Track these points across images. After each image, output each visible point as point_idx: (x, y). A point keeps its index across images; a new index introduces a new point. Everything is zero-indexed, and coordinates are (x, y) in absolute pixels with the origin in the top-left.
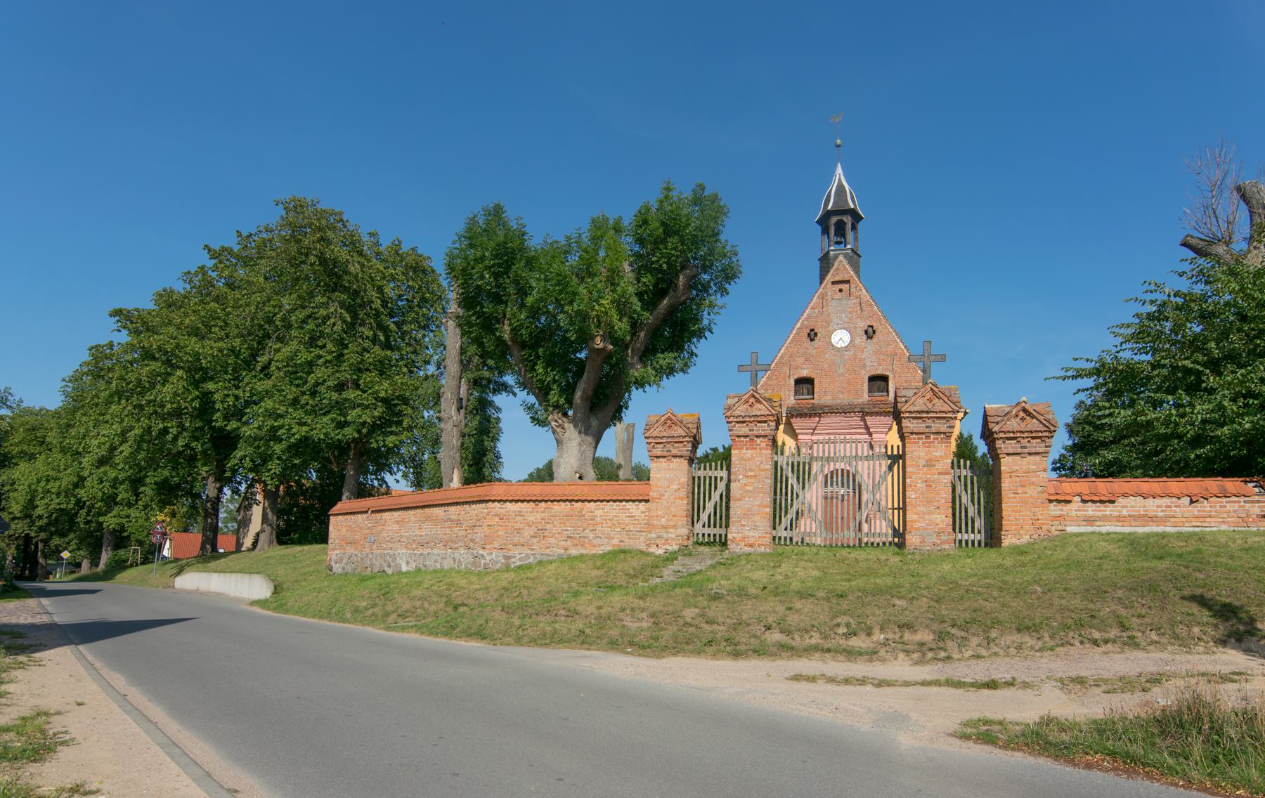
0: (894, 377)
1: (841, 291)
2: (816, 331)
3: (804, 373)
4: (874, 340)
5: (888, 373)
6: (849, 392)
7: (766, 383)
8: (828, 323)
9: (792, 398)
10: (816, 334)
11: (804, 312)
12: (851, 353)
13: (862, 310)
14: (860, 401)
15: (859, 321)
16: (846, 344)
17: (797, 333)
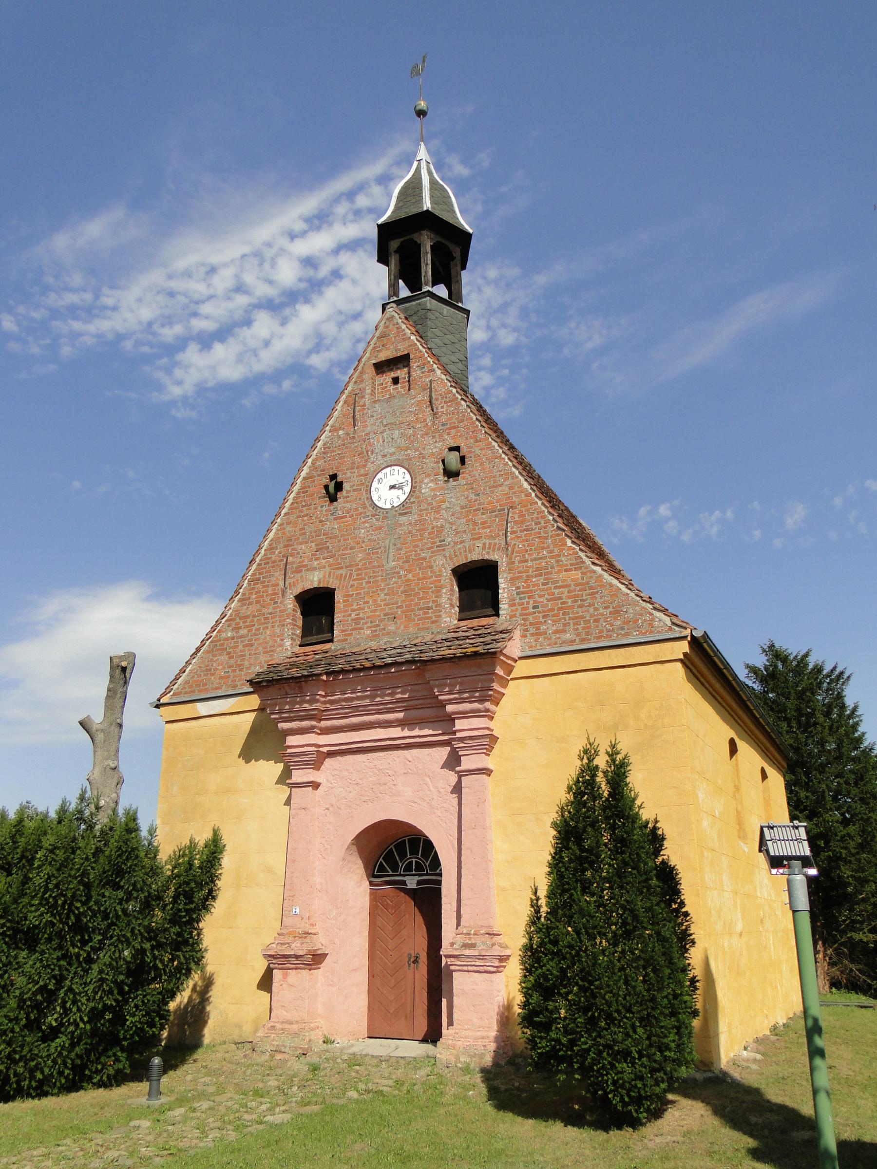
0: (511, 563)
1: (396, 381)
2: (339, 479)
3: (314, 580)
4: (461, 480)
5: (494, 557)
8: (364, 455)
9: (288, 643)
10: (339, 487)
11: (317, 440)
12: (413, 518)
13: (435, 414)
15: (429, 439)
17: (303, 490)
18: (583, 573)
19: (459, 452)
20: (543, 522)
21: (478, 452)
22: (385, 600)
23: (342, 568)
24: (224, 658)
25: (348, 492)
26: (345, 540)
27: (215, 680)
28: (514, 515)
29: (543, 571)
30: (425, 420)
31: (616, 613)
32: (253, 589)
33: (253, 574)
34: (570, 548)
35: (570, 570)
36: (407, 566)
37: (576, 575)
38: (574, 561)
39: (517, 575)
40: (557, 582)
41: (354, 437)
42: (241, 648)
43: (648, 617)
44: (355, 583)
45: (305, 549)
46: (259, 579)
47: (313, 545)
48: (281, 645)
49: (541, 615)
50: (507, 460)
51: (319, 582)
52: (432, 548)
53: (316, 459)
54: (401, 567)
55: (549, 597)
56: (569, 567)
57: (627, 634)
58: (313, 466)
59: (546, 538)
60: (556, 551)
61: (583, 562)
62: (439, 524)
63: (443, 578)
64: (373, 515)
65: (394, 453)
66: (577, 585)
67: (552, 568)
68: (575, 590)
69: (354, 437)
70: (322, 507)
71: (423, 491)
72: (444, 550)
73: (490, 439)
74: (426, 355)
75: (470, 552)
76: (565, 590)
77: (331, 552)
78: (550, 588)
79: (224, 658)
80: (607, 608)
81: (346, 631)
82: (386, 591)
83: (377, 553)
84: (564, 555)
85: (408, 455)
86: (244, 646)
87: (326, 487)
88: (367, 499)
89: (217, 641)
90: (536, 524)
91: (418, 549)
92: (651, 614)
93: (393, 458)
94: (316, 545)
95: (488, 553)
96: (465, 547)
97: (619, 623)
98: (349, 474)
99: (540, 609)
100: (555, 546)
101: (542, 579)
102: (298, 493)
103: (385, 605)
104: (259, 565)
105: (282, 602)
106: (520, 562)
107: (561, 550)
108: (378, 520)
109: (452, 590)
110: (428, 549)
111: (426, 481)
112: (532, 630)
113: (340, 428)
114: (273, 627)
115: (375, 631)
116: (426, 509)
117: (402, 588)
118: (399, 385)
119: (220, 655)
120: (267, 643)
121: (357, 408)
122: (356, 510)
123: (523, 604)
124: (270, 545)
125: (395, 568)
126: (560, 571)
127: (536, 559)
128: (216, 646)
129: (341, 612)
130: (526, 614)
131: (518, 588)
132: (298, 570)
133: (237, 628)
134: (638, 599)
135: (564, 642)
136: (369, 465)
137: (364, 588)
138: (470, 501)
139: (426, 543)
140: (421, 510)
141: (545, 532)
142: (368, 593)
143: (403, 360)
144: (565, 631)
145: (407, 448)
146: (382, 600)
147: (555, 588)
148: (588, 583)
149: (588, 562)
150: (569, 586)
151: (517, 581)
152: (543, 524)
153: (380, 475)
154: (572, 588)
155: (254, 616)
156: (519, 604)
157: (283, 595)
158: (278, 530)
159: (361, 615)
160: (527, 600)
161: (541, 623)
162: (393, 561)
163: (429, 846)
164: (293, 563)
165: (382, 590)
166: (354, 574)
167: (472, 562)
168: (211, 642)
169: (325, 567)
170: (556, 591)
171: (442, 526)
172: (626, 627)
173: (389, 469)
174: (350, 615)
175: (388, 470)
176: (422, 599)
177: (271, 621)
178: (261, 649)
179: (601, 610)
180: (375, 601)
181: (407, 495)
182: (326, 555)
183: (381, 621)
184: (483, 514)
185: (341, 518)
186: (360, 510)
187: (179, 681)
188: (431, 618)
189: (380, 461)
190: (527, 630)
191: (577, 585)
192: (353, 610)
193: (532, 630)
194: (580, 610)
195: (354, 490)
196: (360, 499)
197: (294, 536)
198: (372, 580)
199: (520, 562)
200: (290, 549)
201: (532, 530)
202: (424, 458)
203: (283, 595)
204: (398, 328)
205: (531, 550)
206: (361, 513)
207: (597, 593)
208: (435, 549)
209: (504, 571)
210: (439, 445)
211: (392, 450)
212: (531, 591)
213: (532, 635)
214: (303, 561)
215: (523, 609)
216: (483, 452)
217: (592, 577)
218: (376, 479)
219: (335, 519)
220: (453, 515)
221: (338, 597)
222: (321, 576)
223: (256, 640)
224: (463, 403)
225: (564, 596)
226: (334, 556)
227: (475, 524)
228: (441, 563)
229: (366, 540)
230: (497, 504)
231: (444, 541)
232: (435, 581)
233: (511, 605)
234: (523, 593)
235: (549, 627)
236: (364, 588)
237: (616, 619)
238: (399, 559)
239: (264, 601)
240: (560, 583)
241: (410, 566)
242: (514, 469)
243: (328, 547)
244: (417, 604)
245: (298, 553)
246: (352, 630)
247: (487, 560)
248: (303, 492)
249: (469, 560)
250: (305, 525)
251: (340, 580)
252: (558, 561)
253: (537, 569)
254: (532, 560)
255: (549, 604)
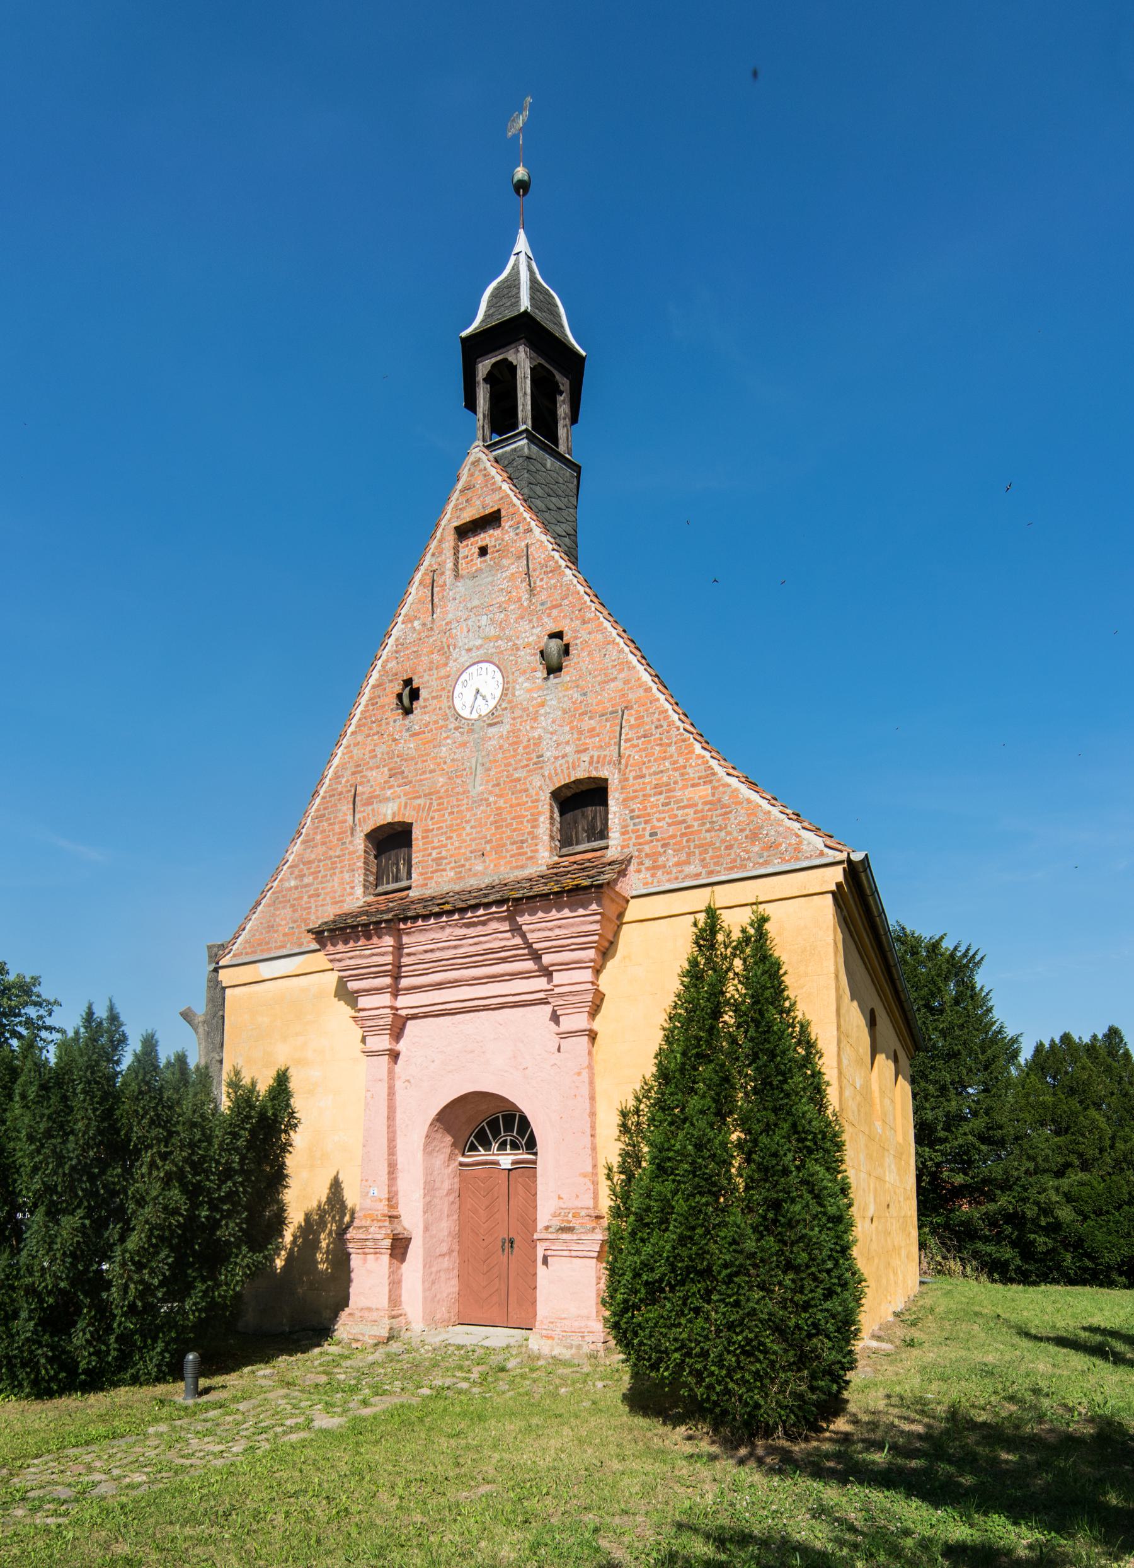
1: (483, 551)
2: (415, 685)
3: (387, 813)
4: (565, 676)
5: (603, 773)
6: (499, 848)
7: (300, 857)
8: (445, 651)
9: (359, 891)
10: (415, 695)
12: (504, 729)
13: (532, 590)
14: (531, 871)
15: (524, 625)
16: (492, 703)
17: (373, 701)
18: (714, 788)
19: (562, 639)
20: (665, 724)
21: (587, 637)
22: (471, 834)
23: (420, 797)
24: (287, 912)
25: (425, 700)
26: (424, 761)
27: (278, 937)
28: (630, 718)
29: (664, 789)
30: (520, 599)
31: (754, 836)
32: (317, 827)
33: (317, 810)
34: (699, 756)
35: (698, 785)
36: (497, 790)
37: (705, 791)
38: (703, 774)
39: (632, 794)
40: (682, 801)
41: (432, 629)
42: (306, 899)
43: (794, 840)
44: (436, 815)
45: (377, 777)
46: (324, 815)
47: (386, 769)
48: (352, 894)
49: (659, 844)
50: (622, 645)
51: (394, 815)
52: (527, 766)
53: (387, 661)
54: (491, 792)
55: (670, 821)
56: (696, 781)
57: (766, 863)
58: (384, 671)
59: (669, 745)
60: (681, 761)
61: (714, 774)
62: (536, 735)
63: (541, 803)
64: (456, 729)
65: (481, 646)
66: (705, 803)
67: (676, 783)
68: (702, 811)
69: (432, 629)
70: (395, 721)
71: (517, 693)
72: (541, 768)
73: (602, 619)
74: (522, 509)
75: (574, 768)
76: (690, 811)
77: (407, 777)
78: (672, 810)
79: (287, 912)
80: (742, 830)
81: (426, 873)
82: (472, 823)
83: (461, 776)
84: (691, 766)
85: (499, 647)
86: (310, 897)
87: (400, 696)
88: (449, 708)
89: (279, 892)
90: (657, 727)
91: (510, 768)
92: (797, 836)
93: (481, 652)
94: (390, 770)
95: (596, 769)
96: (567, 762)
97: (756, 849)
98: (426, 678)
99: (659, 836)
100: (680, 754)
101: (662, 798)
102: (367, 706)
103: (471, 840)
104: (324, 798)
105: (351, 842)
106: (635, 778)
107: (687, 760)
108: (462, 733)
109: (552, 818)
110: (523, 767)
111: (520, 680)
112: (648, 863)
113: (416, 618)
114: (342, 872)
115: (460, 872)
116: (521, 717)
117: (492, 819)
118: (488, 557)
119: (284, 908)
120: (335, 892)
121: (436, 590)
122: (436, 722)
123: (638, 831)
124: (335, 773)
125: (482, 793)
126: (684, 787)
127: (655, 773)
128: (278, 898)
129: (420, 851)
130: (640, 844)
131: (633, 811)
132: (369, 803)
133: (301, 876)
134: (784, 816)
135: (686, 877)
136: (451, 663)
137: (446, 821)
138: (574, 703)
139: (520, 761)
140: (514, 719)
141: (669, 738)
142: (451, 826)
143: (491, 520)
144: (689, 863)
145: (498, 638)
146: (468, 835)
147: (679, 808)
148: (719, 800)
149: (721, 772)
150: (696, 805)
151: (631, 803)
152: (665, 727)
153: (464, 676)
154: (700, 807)
155: (320, 861)
156: (634, 831)
157: (352, 834)
158: (344, 754)
159: (443, 854)
160: (643, 825)
161: (660, 854)
162: (481, 785)
163: (524, 1123)
164: (363, 793)
165: (467, 822)
166: (435, 803)
167: (578, 782)
168: (273, 893)
169: (399, 797)
170: (680, 813)
171: (540, 738)
172: (765, 854)
173: (475, 667)
174: (430, 854)
175: (473, 669)
176: (515, 830)
177: (339, 865)
178: (328, 900)
179: (735, 834)
180: (459, 835)
181: (497, 700)
182: (401, 781)
183: (467, 859)
184: (591, 718)
185: (417, 734)
186: (441, 723)
187: (239, 941)
188: (526, 853)
189: (464, 658)
190: (641, 863)
191: (705, 803)
192: (434, 848)
193: (648, 863)
194: (708, 835)
195: (434, 698)
196: (440, 709)
197: (363, 759)
198: (455, 810)
199: (635, 778)
200: (358, 776)
201: (652, 735)
202: (518, 649)
203: (352, 834)
204: (485, 476)
205: (649, 761)
206: (441, 727)
207: (731, 812)
208: (531, 767)
209: (616, 790)
210: (536, 631)
211: (479, 642)
212: (649, 814)
213: (648, 869)
214: (374, 791)
215: (638, 837)
216: (593, 636)
217: (724, 793)
218: (459, 682)
219: (411, 736)
220: (553, 722)
221: (416, 833)
222: (396, 808)
223: (323, 888)
224: (568, 571)
225: (689, 818)
226: (411, 782)
227: (580, 732)
228: (538, 784)
229: (448, 761)
230: (609, 705)
231: (542, 756)
232: (531, 808)
233: (623, 834)
234: (639, 817)
235: (670, 858)
236: (446, 821)
237: (753, 844)
238: (488, 781)
239: (331, 841)
240: (685, 803)
241: (501, 790)
242: (631, 657)
243: (403, 772)
244: (509, 837)
245: (368, 781)
246: (433, 872)
247: (595, 778)
248: (373, 704)
249: (573, 779)
250: (375, 745)
251: (418, 812)
252: (682, 775)
253: (656, 786)
254: (650, 775)
255: (671, 829)
